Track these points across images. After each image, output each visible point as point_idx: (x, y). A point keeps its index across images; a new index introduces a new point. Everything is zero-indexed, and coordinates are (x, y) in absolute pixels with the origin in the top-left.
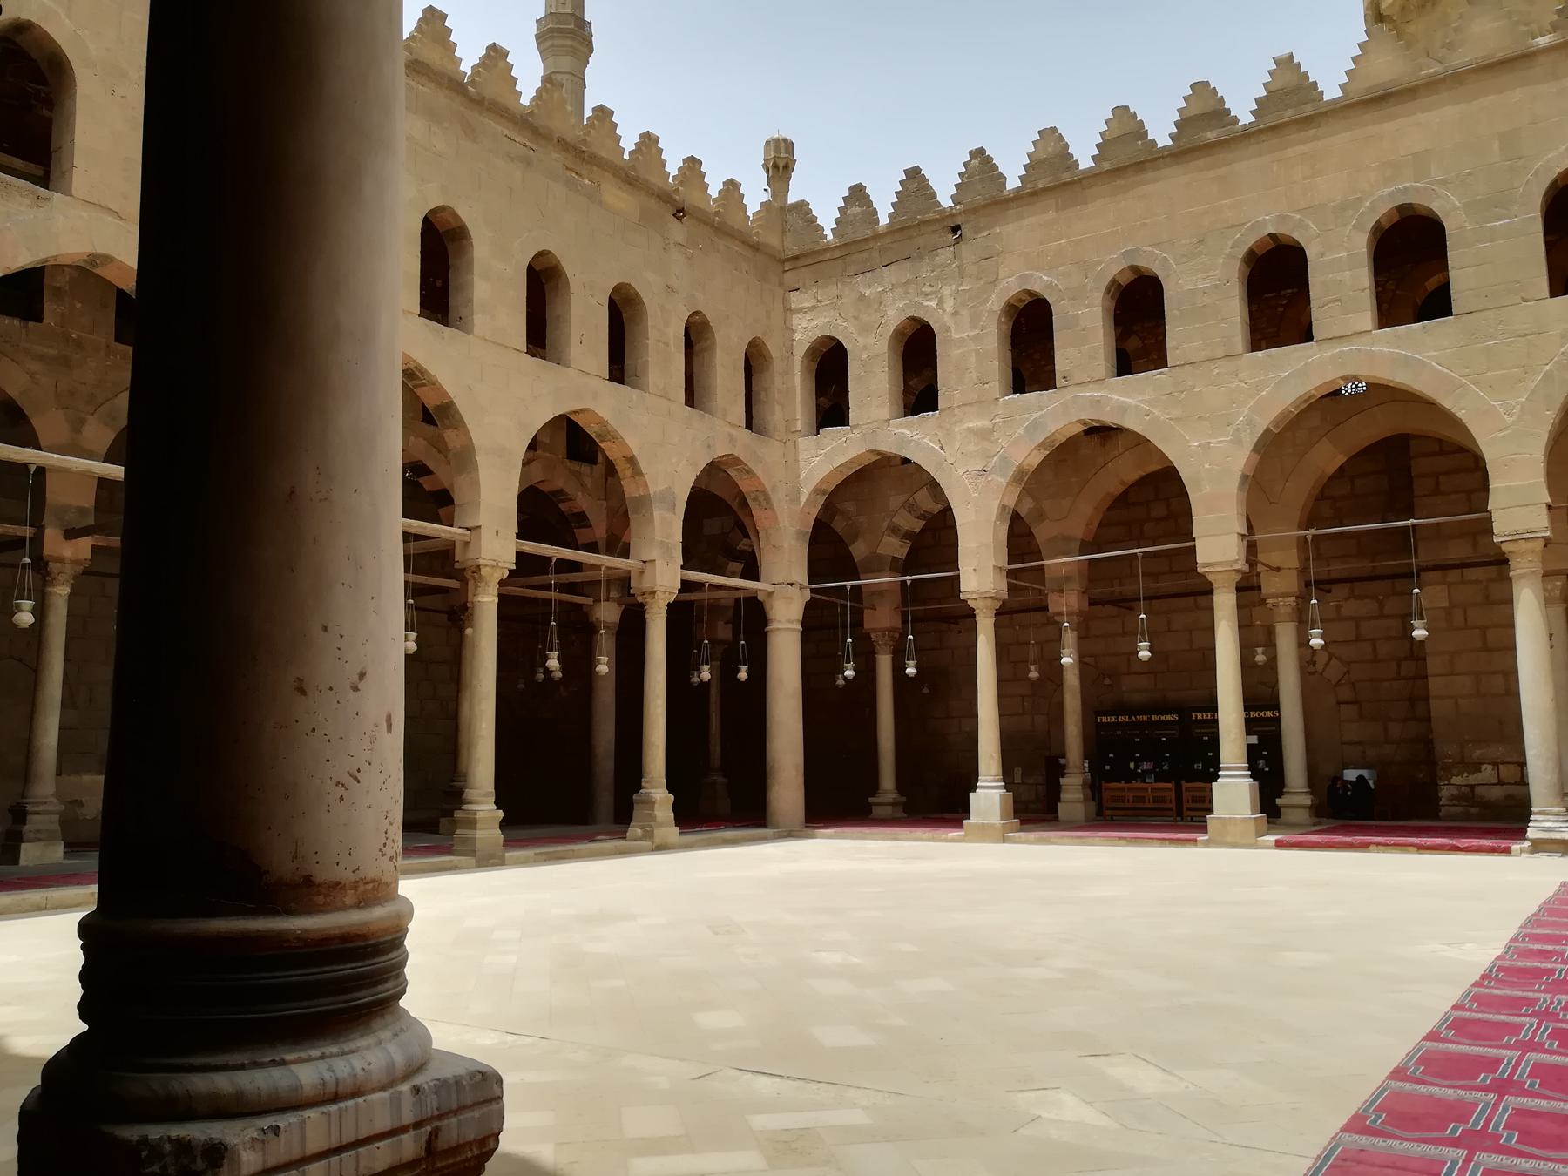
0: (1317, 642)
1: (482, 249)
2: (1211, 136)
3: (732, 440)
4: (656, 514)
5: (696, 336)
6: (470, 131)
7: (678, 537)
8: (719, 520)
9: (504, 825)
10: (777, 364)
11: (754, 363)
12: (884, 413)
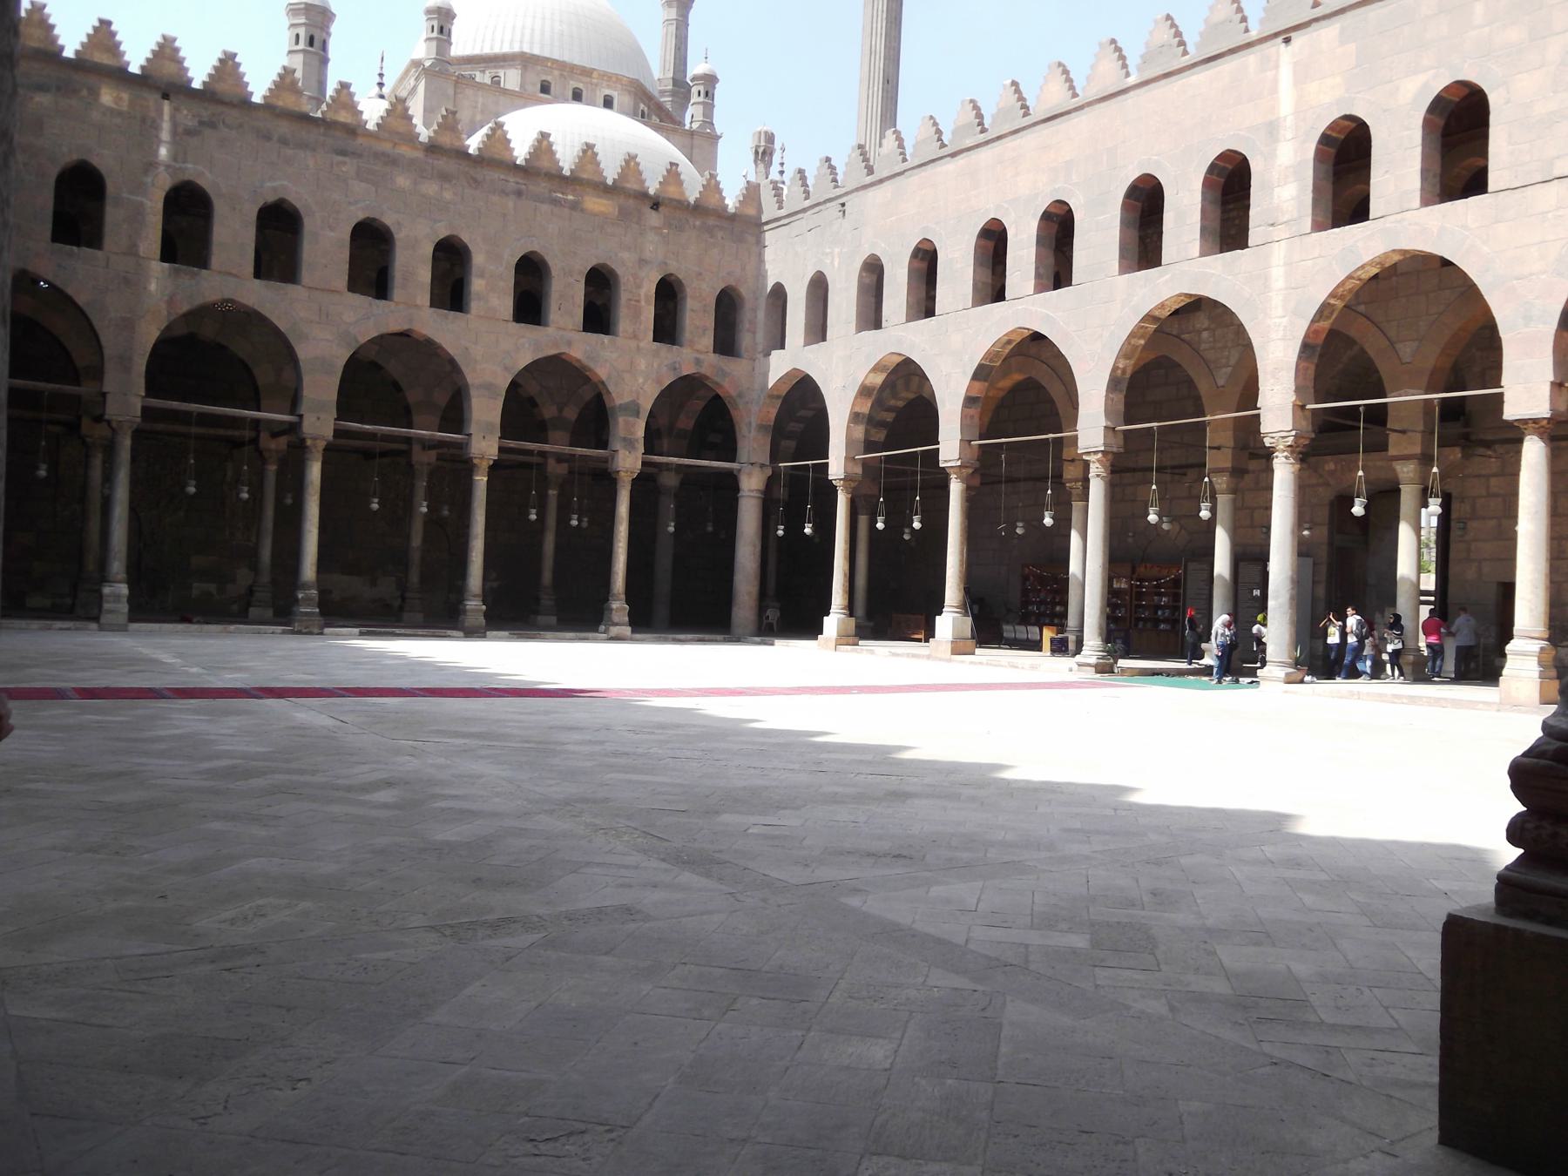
0: (880, 526)
1: (478, 259)
2: (969, 143)
3: (698, 362)
4: (621, 420)
5: (668, 293)
6: (476, 183)
7: (641, 433)
8: (699, 418)
9: (487, 615)
10: (748, 305)
11: (727, 306)
12: (801, 340)
